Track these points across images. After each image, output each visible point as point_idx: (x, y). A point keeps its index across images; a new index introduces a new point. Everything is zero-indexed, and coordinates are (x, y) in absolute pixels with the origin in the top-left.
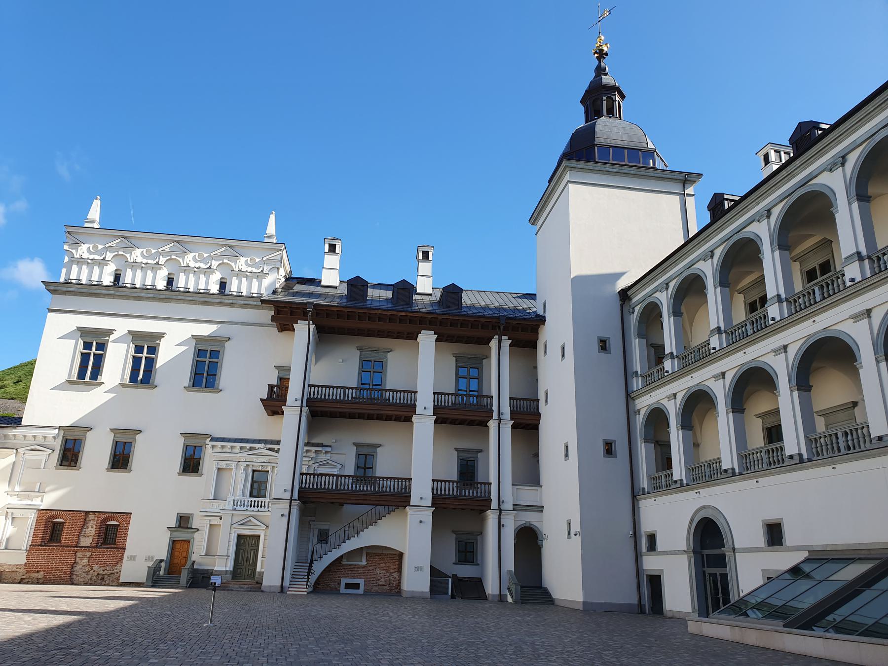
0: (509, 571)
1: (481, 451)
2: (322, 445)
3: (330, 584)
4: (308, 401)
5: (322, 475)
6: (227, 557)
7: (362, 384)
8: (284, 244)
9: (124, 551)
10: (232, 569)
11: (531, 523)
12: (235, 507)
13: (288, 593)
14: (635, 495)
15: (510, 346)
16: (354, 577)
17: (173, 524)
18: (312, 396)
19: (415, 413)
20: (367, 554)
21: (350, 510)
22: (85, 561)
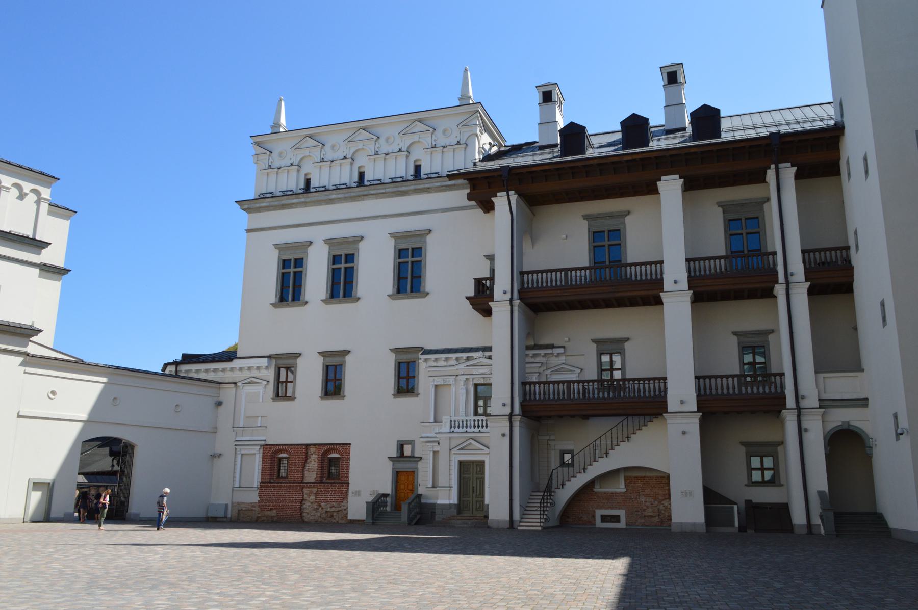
0: (821, 494)
1: (772, 331)
2: (552, 346)
3: (582, 517)
4: (520, 292)
5: (559, 382)
6: (449, 488)
7: (595, 263)
8: (480, 103)
9: (348, 486)
10: (456, 503)
11: (852, 423)
12: (453, 429)
13: (519, 528)
15: (797, 177)
16: (612, 508)
18: (526, 286)
19: (662, 290)
20: (626, 479)
22: (312, 497)
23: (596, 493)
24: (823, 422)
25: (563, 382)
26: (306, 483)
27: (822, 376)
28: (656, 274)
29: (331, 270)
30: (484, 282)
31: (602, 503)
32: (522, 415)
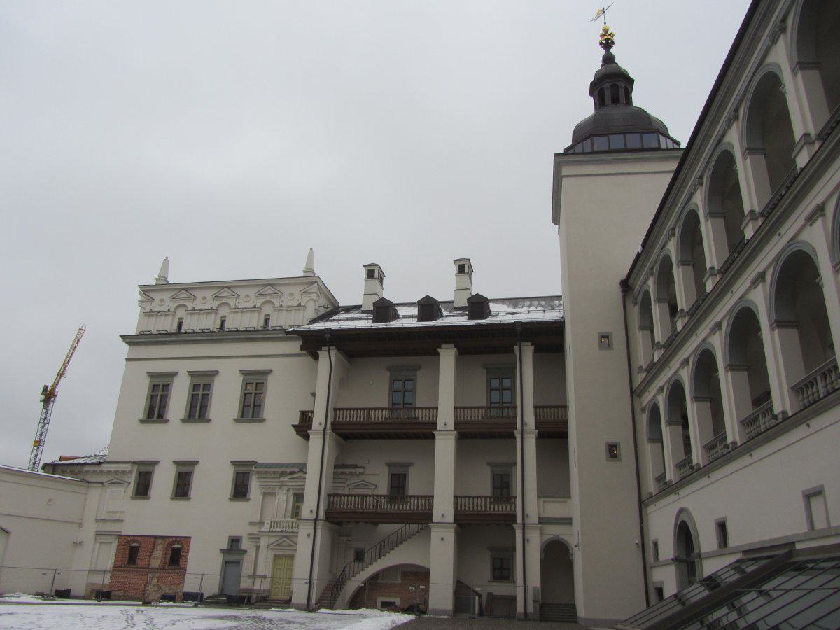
2: (356, 467)
4: (332, 424)
7: (393, 404)
11: (560, 536)
14: (642, 505)
17: (225, 546)
18: (337, 420)
19: (435, 429)
21: (387, 529)
22: (155, 581)
24: (540, 534)
25: (359, 496)
26: (151, 569)
27: (542, 500)
28: (433, 417)
29: (191, 395)
30: (310, 414)
32: (325, 519)
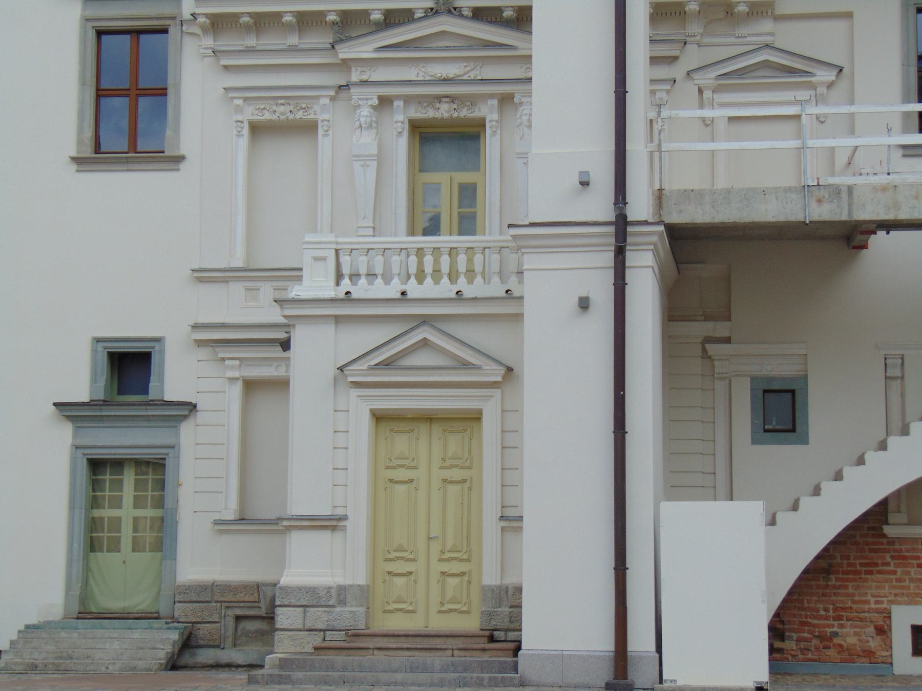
3: (836, 634)
12: (346, 283)
23: (892, 542)
31: (911, 580)
